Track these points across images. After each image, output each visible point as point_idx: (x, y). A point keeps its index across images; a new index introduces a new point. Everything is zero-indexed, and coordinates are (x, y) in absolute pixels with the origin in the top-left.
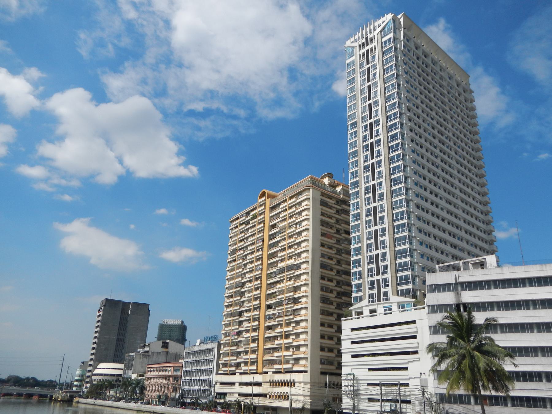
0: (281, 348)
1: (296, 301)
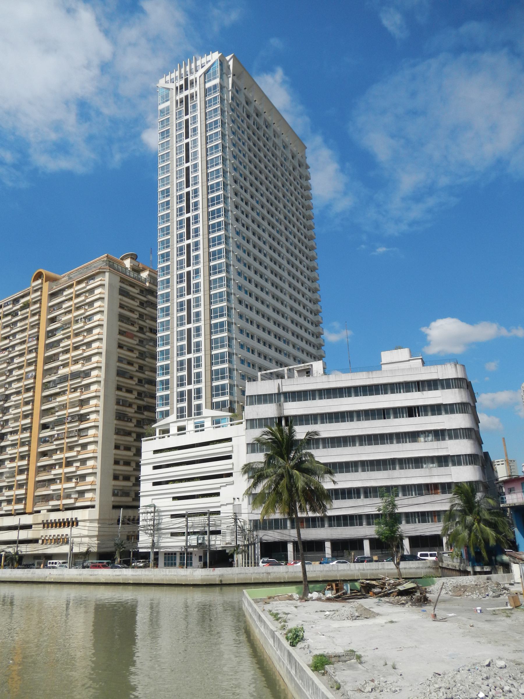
0: (60, 479)
1: (83, 418)
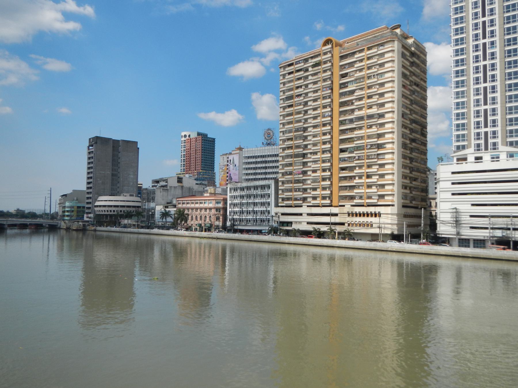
1: (380, 146)
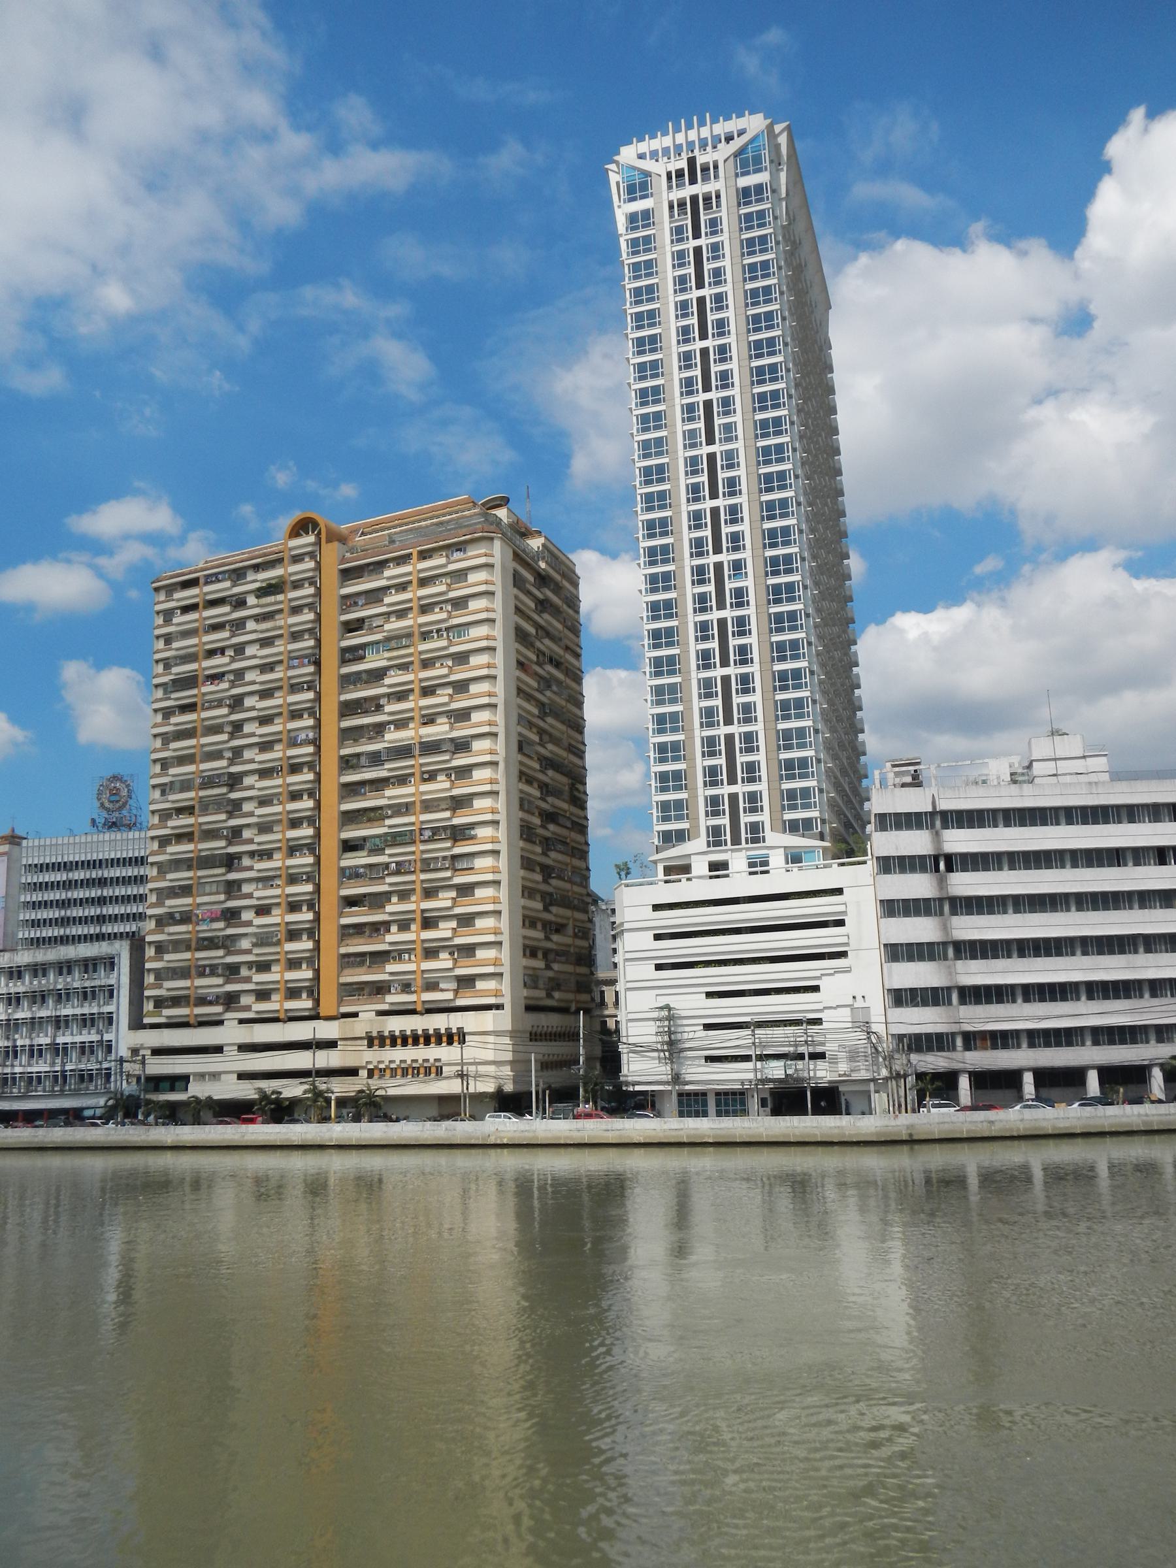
1: (459, 834)
